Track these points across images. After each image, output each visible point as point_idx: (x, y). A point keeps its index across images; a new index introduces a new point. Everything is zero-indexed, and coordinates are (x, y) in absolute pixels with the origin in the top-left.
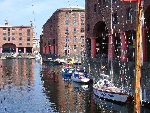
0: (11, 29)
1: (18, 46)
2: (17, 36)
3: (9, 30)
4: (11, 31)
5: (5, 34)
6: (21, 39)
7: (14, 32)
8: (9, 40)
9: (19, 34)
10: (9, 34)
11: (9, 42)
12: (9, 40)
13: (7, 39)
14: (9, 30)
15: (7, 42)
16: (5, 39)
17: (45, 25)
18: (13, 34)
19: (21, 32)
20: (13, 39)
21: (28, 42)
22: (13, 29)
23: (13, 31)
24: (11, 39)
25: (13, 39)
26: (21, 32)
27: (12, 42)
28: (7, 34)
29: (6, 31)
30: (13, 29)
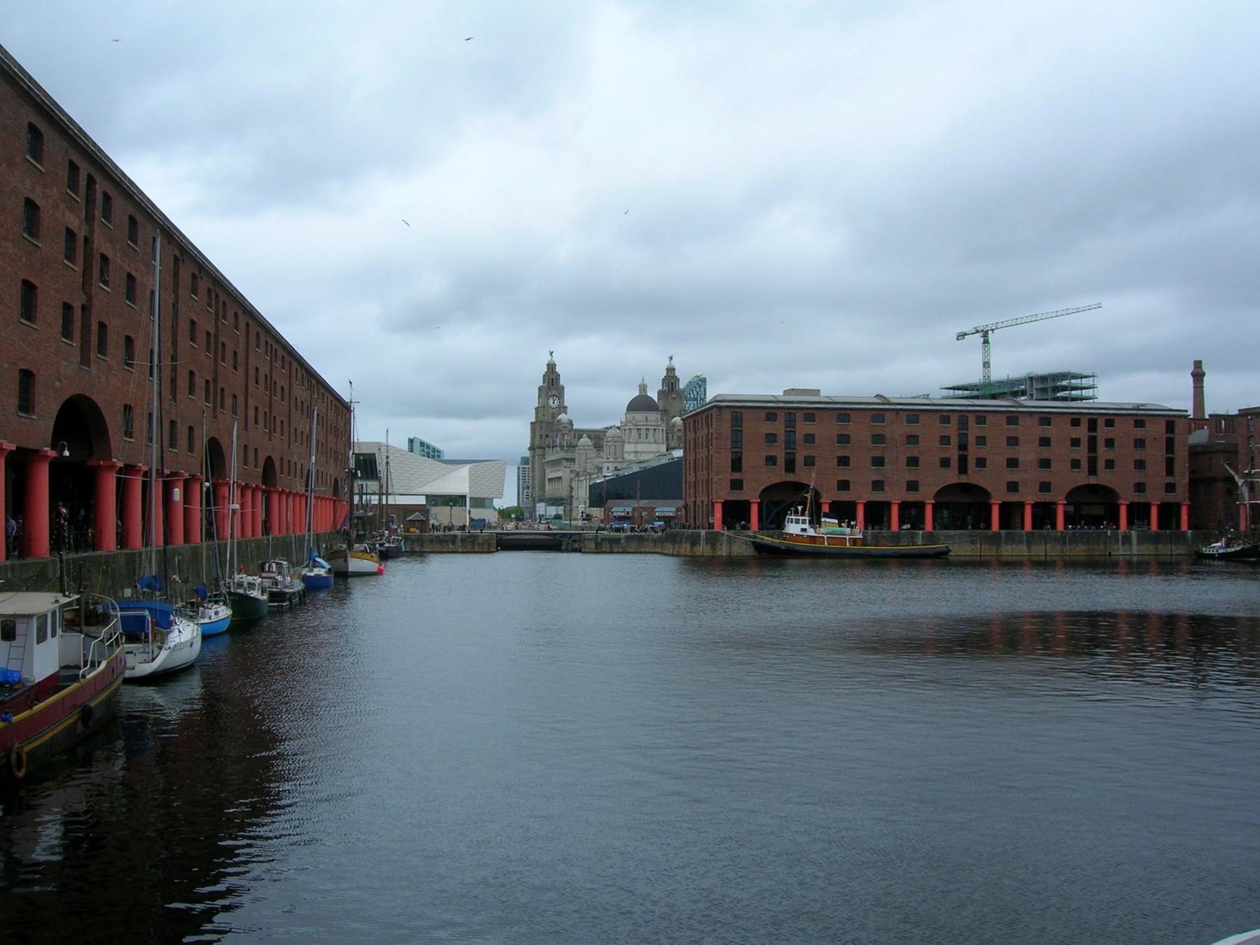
0: (1101, 422)
1: (1127, 496)
2: (1125, 454)
3: (1093, 425)
4: (1102, 432)
5: (1075, 442)
9: (1132, 444)
11: (1093, 480)
12: (1093, 470)
13: (1085, 465)
14: (1093, 425)
15: (1081, 478)
16: (1076, 464)
18: (1110, 443)
19: (1139, 433)
20: (1110, 464)
21: (1170, 480)
22: (1110, 423)
24: (1101, 464)
25: (1110, 464)
26: (1139, 433)
27: (1104, 478)
29: (1082, 432)
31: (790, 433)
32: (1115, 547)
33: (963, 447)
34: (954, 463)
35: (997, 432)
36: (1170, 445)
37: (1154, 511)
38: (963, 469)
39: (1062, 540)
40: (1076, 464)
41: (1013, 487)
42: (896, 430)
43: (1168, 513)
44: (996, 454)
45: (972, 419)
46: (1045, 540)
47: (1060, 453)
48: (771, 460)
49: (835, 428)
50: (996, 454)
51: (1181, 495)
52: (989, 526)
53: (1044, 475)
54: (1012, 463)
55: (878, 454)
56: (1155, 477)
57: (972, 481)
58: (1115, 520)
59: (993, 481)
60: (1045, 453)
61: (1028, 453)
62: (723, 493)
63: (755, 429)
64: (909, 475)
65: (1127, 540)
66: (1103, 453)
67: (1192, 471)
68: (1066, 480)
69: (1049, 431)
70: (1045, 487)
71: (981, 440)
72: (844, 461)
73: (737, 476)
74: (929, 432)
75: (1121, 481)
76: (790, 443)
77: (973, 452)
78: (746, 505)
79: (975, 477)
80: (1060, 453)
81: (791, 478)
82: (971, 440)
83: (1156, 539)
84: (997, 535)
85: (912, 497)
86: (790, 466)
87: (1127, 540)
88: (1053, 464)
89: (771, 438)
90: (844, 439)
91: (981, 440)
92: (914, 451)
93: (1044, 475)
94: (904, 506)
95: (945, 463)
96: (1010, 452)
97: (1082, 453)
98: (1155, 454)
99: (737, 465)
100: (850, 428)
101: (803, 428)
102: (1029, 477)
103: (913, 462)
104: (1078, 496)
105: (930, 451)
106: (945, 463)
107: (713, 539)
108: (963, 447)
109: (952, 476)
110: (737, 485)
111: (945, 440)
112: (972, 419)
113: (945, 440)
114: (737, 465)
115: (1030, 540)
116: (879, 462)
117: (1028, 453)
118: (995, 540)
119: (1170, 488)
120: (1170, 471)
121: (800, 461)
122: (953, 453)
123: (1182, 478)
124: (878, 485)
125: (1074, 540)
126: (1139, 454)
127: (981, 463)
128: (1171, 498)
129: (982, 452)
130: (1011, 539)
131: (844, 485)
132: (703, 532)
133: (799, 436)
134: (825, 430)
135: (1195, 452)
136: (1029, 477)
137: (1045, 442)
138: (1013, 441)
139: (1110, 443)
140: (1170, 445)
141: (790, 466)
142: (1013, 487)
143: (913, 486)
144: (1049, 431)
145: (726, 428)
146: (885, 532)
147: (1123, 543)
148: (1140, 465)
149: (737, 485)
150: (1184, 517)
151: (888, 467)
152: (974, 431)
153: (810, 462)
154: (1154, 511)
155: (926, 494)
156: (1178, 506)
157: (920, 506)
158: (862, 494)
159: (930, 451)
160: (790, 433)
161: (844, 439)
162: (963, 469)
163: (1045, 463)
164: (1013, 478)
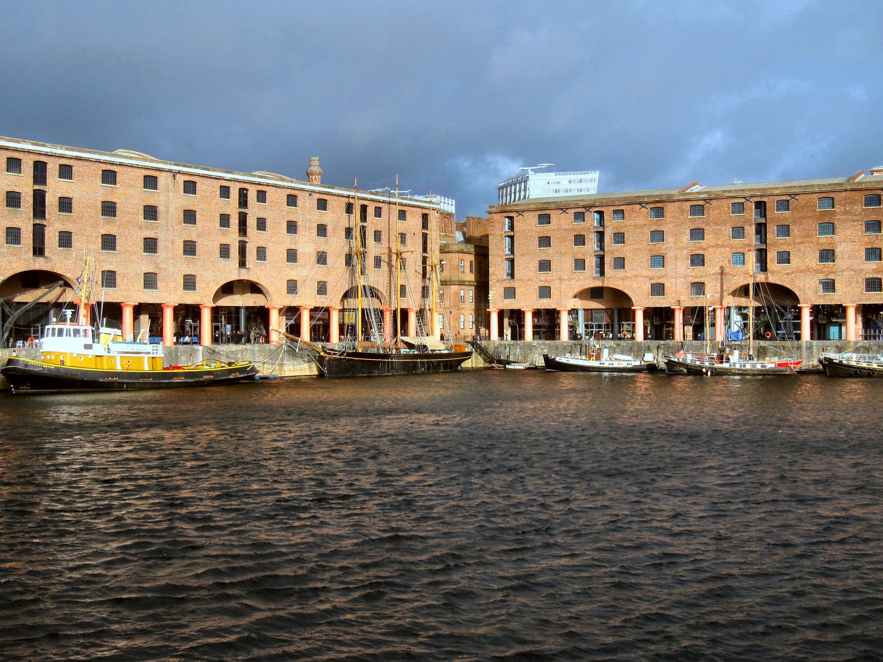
48: (13, 235)
57: (253, 278)
64: (185, 266)
81: (39, 264)
82: (251, 222)
88: (329, 261)
93: (320, 273)
102: (306, 272)
103: (190, 248)
106: (225, 251)
127: (261, 253)
133: (51, 201)
142: (292, 287)
143: (189, 283)
144: (326, 217)
151: (162, 253)
153: (65, 240)
155: (203, 297)
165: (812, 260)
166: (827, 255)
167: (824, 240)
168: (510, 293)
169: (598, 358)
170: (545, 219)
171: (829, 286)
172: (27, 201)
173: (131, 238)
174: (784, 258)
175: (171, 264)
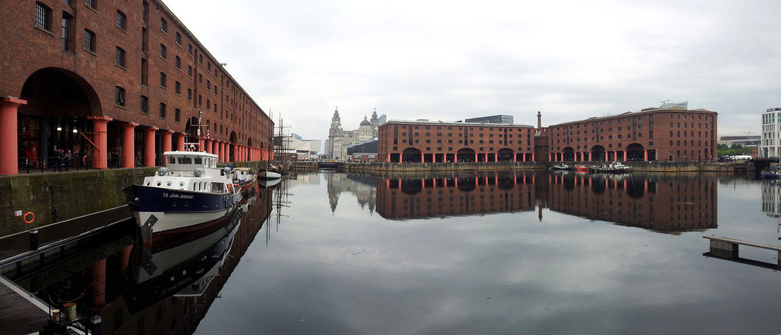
0: (508, 130)
2: (515, 139)
3: (506, 130)
4: (509, 132)
5: (501, 136)
6: (520, 142)
7: (511, 133)
8: (506, 144)
10: (506, 136)
11: (506, 147)
12: (506, 144)
13: (503, 142)
15: (503, 146)
16: (501, 142)
17: (581, 126)
18: (511, 136)
19: (519, 133)
20: (511, 142)
21: (529, 146)
22: (511, 130)
23: (511, 133)
24: (508, 142)
25: (511, 142)
26: (519, 133)
27: (509, 146)
28: (503, 136)
29: (502, 132)
30: (511, 130)
31: (411, 133)
32: (512, 167)
33: (466, 137)
34: (463, 142)
35: (476, 132)
36: (529, 136)
37: (524, 156)
38: (466, 143)
39: (497, 165)
40: (501, 142)
41: (482, 149)
42: (445, 132)
43: (528, 156)
44: (477, 139)
45: (469, 128)
46: (492, 165)
47: (496, 139)
49: (425, 131)
50: (477, 139)
51: (532, 151)
52: (474, 161)
53: (491, 145)
54: (481, 142)
55: (440, 139)
56: (524, 146)
58: (512, 157)
59: (475, 147)
60: (491, 139)
61: (486, 139)
62: (391, 151)
63: (401, 131)
65: (516, 164)
66: (509, 139)
67: (536, 144)
68: (497, 147)
69: (493, 132)
70: (491, 149)
71: (472, 135)
72: (428, 141)
73: (396, 146)
74: (456, 132)
75: (514, 147)
76: (411, 135)
77: (469, 139)
78: (398, 155)
79: (470, 146)
80: (496, 139)
81: (411, 146)
82: (469, 135)
83: (525, 164)
84: (477, 163)
85: (450, 152)
86: (411, 143)
87: (516, 164)
89: (404, 134)
90: (428, 134)
91: (472, 135)
92: (450, 138)
93: (491, 145)
94: (448, 155)
95: (461, 142)
96: (480, 139)
97: (502, 139)
98: (524, 139)
99: (396, 142)
100: (430, 131)
101: (415, 131)
102: (486, 146)
103: (450, 141)
104: (501, 151)
105: (455, 138)
107: (387, 165)
108: (466, 137)
109: (463, 146)
110: (395, 148)
111: (460, 135)
112: (469, 128)
113: (460, 135)
114: (396, 142)
115: (487, 165)
116: (439, 141)
117: (486, 139)
118: (476, 165)
119: (529, 149)
120: (529, 144)
121: (414, 141)
122: (463, 139)
123: (532, 146)
124: (439, 149)
125: (501, 164)
126: (520, 139)
127: (472, 142)
128: (529, 152)
129: (472, 138)
130: (481, 165)
131: (428, 149)
132: (384, 163)
133: (413, 133)
134: (422, 131)
135: (536, 139)
136: (486, 146)
137: (491, 135)
138: (481, 135)
139: (511, 136)
140: (529, 136)
141: (411, 143)
143: (450, 149)
144: (493, 132)
145: (392, 130)
146: (442, 163)
147: (515, 166)
148: (520, 142)
149: (395, 148)
150: (533, 157)
152: (469, 132)
153: (417, 141)
154: (524, 156)
155: (455, 152)
156: (531, 154)
157: (453, 155)
158: (434, 152)
159: (455, 138)
160: (411, 133)
161: (428, 134)
162: (466, 143)
163: (491, 142)
164: (482, 146)
165: (607, 139)
166: (610, 137)
167: (609, 133)
168: (552, 148)
169: (561, 166)
170: (558, 129)
171: (610, 145)
172: (408, 134)
173: (434, 141)
174: (602, 138)
175: (445, 146)
